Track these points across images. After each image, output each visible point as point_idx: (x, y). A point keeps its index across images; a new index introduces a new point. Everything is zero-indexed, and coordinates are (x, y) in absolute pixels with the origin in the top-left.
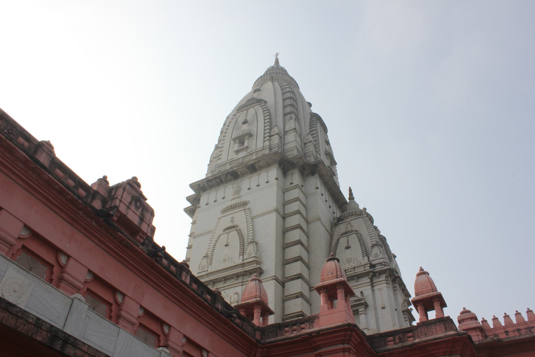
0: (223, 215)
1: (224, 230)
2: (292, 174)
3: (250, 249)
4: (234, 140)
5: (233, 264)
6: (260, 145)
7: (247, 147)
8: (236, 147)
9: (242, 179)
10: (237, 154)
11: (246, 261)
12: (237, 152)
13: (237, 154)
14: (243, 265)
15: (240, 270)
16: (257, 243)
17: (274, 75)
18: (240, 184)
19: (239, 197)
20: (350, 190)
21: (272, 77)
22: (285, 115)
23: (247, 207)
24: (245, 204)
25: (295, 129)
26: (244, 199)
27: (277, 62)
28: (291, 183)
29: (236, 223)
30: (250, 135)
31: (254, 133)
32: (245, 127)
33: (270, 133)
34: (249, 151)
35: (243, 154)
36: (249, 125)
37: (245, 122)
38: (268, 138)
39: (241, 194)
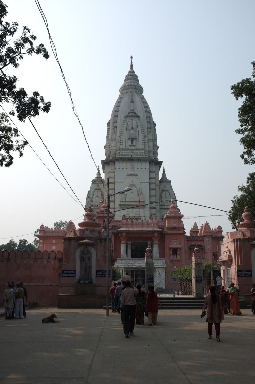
0: (127, 177)
1: (130, 185)
2: (152, 165)
3: (141, 196)
4: (129, 139)
5: (135, 201)
6: (141, 147)
7: (134, 146)
8: (130, 143)
9: (134, 162)
10: (130, 147)
12: (131, 146)
13: (130, 147)
16: (142, 194)
17: (136, 87)
19: (134, 171)
20: (164, 167)
21: (135, 88)
22: (148, 128)
23: (138, 177)
24: (137, 175)
25: (152, 140)
27: (132, 66)
28: (153, 170)
29: (134, 183)
30: (136, 139)
32: (132, 131)
33: (144, 141)
34: (135, 147)
35: (132, 148)
36: (134, 131)
37: (132, 129)
38: (143, 144)
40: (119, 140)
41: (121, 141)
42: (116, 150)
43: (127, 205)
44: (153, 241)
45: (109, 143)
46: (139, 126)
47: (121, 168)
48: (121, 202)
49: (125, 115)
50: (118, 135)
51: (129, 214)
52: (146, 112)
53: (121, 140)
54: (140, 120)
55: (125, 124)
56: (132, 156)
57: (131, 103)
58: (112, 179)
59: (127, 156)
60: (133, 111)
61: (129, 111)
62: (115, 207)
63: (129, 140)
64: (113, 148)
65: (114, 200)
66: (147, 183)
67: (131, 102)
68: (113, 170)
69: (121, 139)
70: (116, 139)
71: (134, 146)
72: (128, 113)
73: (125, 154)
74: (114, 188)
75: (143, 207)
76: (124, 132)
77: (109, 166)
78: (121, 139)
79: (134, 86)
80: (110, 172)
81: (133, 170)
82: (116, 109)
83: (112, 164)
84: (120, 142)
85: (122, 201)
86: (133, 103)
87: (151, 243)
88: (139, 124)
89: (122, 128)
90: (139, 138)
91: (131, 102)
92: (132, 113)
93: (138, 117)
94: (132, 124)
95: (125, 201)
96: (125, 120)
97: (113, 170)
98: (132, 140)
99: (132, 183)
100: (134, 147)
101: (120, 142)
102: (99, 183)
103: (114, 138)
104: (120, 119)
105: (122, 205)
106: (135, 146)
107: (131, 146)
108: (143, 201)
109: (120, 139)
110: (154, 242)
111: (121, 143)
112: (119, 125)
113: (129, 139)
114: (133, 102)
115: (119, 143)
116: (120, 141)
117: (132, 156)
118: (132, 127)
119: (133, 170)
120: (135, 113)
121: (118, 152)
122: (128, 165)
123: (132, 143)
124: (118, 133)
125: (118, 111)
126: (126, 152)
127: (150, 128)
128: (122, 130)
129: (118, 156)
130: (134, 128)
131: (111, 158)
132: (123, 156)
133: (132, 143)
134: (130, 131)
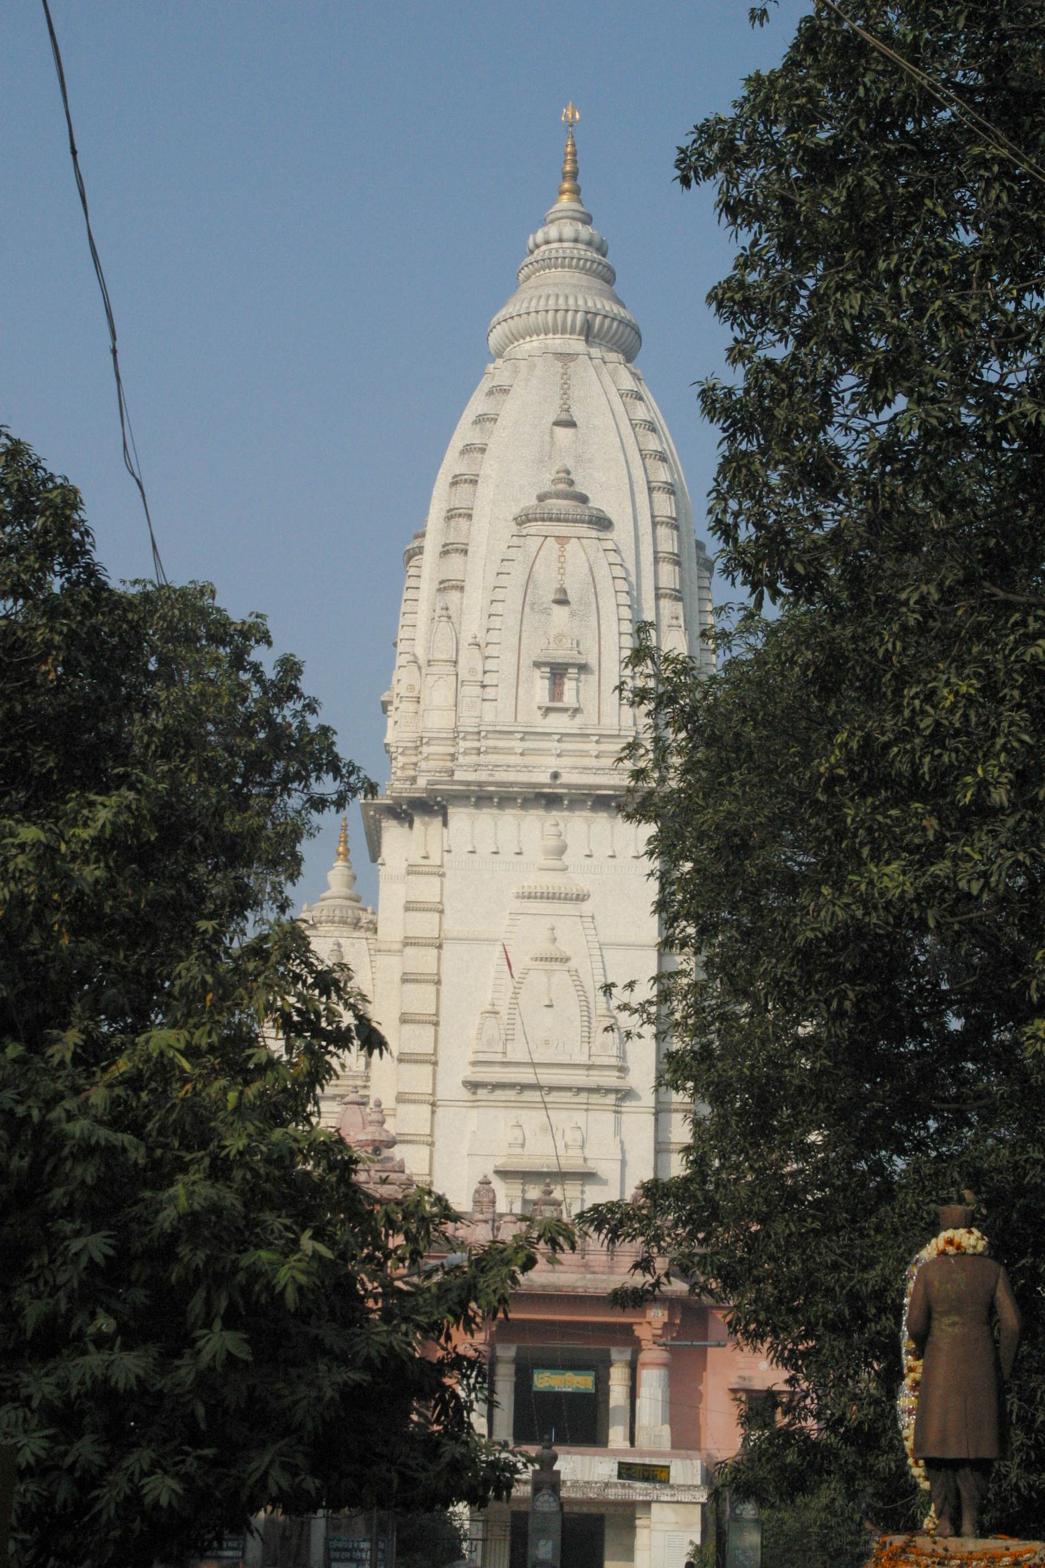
0: (517, 905)
4: (537, 665)
8: (540, 688)
11: (598, 1061)
14: (590, 1067)
15: (580, 1078)
18: (561, 827)
23: (587, 907)
24: (581, 898)
26: (579, 882)
30: (583, 668)
31: (593, 662)
34: (579, 719)
35: (559, 722)
36: (573, 615)
37: (563, 602)
39: (567, 858)
40: (472, 671)
41: (488, 679)
42: (456, 735)
43: (511, 1086)
44: (636, 1346)
45: (411, 688)
46: (605, 586)
47: (485, 848)
48: (475, 1064)
49: (516, 510)
50: (466, 639)
51: (523, 1145)
52: (651, 490)
53: (485, 672)
54: (610, 545)
55: (518, 573)
56: (555, 776)
57: (560, 431)
58: (429, 915)
59: (523, 777)
60: (571, 483)
61: (546, 481)
62: (439, 1096)
63: (537, 673)
64: (439, 721)
65: (435, 1049)
66: (642, 946)
67: (557, 423)
68: (435, 859)
69: (491, 665)
70: (456, 662)
71: (565, 710)
72: (541, 498)
73: (512, 759)
74: (438, 974)
75: (611, 1099)
76: (512, 621)
77: (411, 826)
78: (491, 665)
79: (580, 317)
80: (412, 870)
81: (557, 864)
82: (461, 467)
83: (426, 825)
84: (484, 686)
85: (482, 1057)
86: (570, 431)
87: (627, 1356)
88: (603, 573)
89: (499, 594)
90: (603, 666)
91: (557, 423)
92: (558, 495)
93: (603, 523)
94: (562, 570)
95: (499, 1058)
96: (515, 541)
97: (435, 859)
98: (557, 672)
99: (545, 948)
100: (573, 716)
101: (484, 686)
102: (346, 931)
103: (444, 657)
104: (489, 530)
105: (483, 1085)
106: (577, 711)
107: (548, 710)
108: (614, 1061)
109: (480, 670)
110: (644, 1357)
111: (490, 693)
112: (477, 570)
113: (537, 665)
114: (571, 424)
115: (477, 690)
116: (479, 677)
117: (555, 776)
118: (565, 592)
119: (557, 864)
120: (583, 499)
121: (469, 744)
122: (533, 828)
123: (556, 692)
124: (472, 625)
125: (474, 482)
126: (518, 746)
127: (677, 596)
128: (498, 608)
129: (471, 777)
130: (572, 596)
131: (422, 782)
132: (501, 776)
133: (556, 692)
134: (546, 612)
